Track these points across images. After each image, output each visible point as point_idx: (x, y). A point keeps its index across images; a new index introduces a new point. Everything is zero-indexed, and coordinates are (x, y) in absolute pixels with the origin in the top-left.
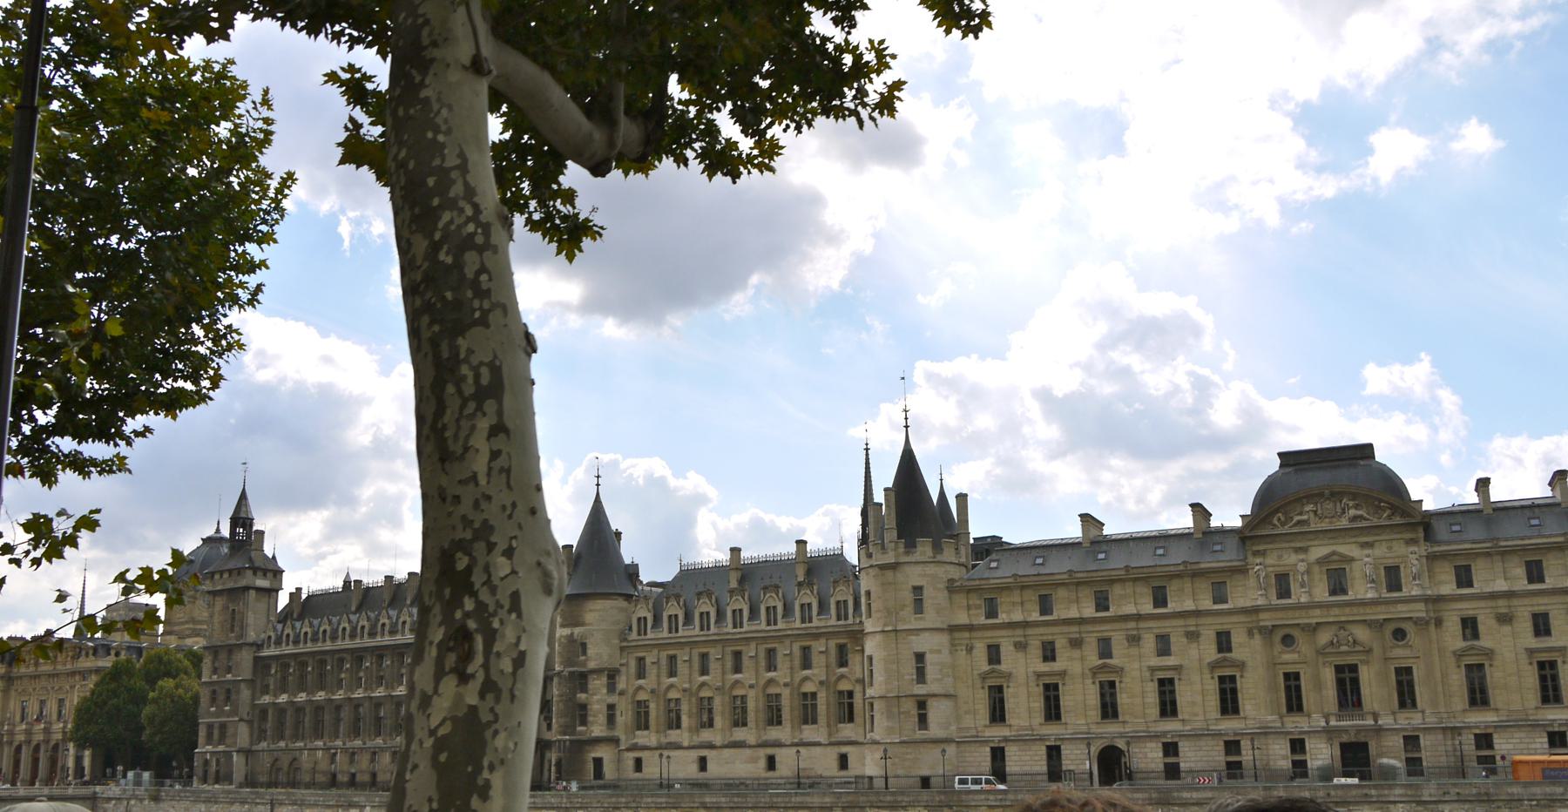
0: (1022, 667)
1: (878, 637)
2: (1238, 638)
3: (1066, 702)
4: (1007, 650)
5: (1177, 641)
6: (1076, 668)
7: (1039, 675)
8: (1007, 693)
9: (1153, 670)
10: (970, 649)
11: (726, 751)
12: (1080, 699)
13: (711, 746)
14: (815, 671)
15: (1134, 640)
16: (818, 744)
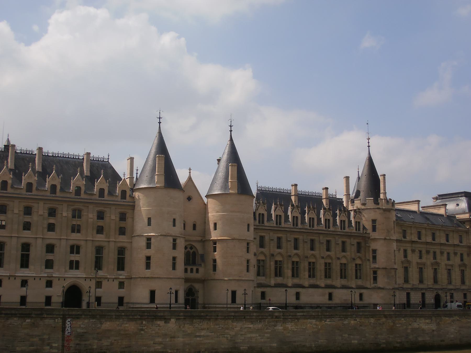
0: (414, 258)
2: (465, 257)
3: (425, 275)
4: (409, 252)
5: (452, 255)
6: (429, 263)
7: (418, 263)
8: (410, 270)
9: (446, 265)
10: (399, 250)
11: (310, 289)
12: (429, 273)
13: (302, 287)
14: (348, 253)
15: (442, 253)
16: (352, 288)
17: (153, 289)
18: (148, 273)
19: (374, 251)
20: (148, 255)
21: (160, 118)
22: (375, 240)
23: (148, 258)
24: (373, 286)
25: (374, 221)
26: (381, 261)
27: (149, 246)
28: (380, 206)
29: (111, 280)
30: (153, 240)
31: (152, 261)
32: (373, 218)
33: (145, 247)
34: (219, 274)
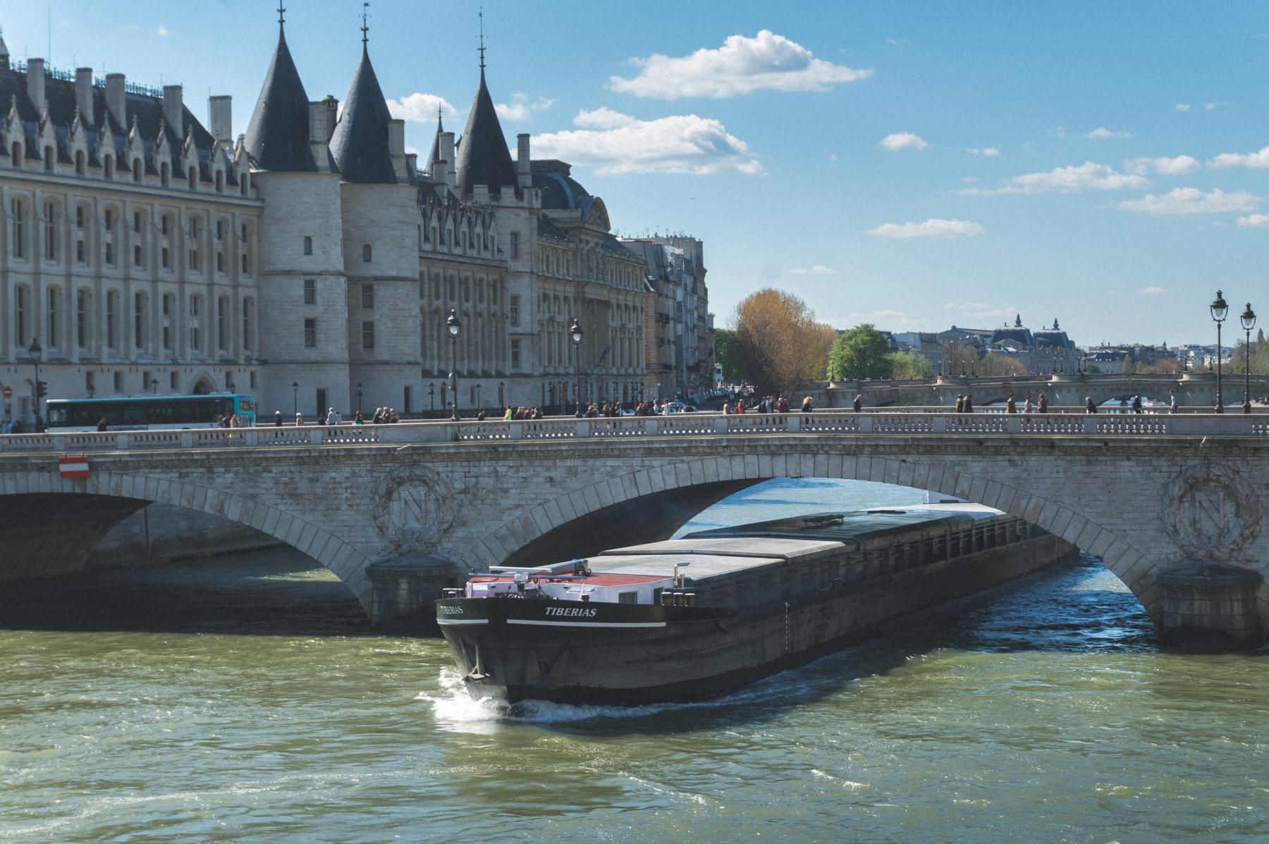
1: (526, 279)
14: (485, 304)
17: (322, 387)
18: (312, 355)
19: (515, 299)
20: (311, 316)
21: (281, 11)
22: (518, 274)
23: (310, 323)
24: (512, 371)
25: (515, 235)
26: (528, 320)
27: (310, 297)
28: (525, 204)
29: (242, 368)
30: (319, 285)
31: (321, 327)
32: (515, 229)
33: (303, 301)
34: (382, 353)
